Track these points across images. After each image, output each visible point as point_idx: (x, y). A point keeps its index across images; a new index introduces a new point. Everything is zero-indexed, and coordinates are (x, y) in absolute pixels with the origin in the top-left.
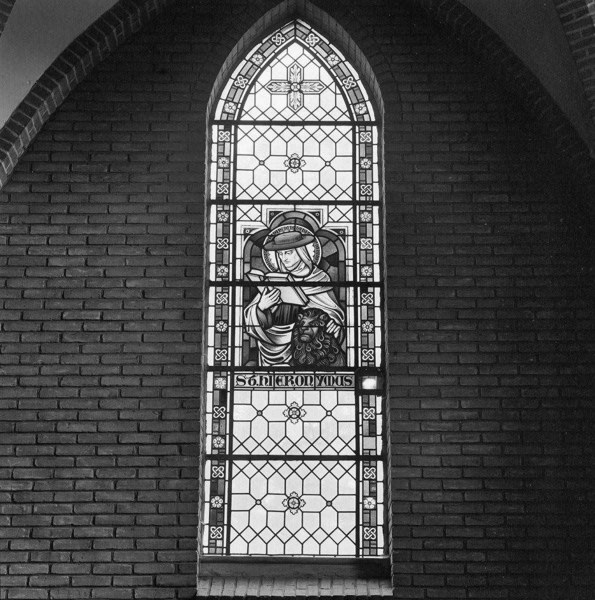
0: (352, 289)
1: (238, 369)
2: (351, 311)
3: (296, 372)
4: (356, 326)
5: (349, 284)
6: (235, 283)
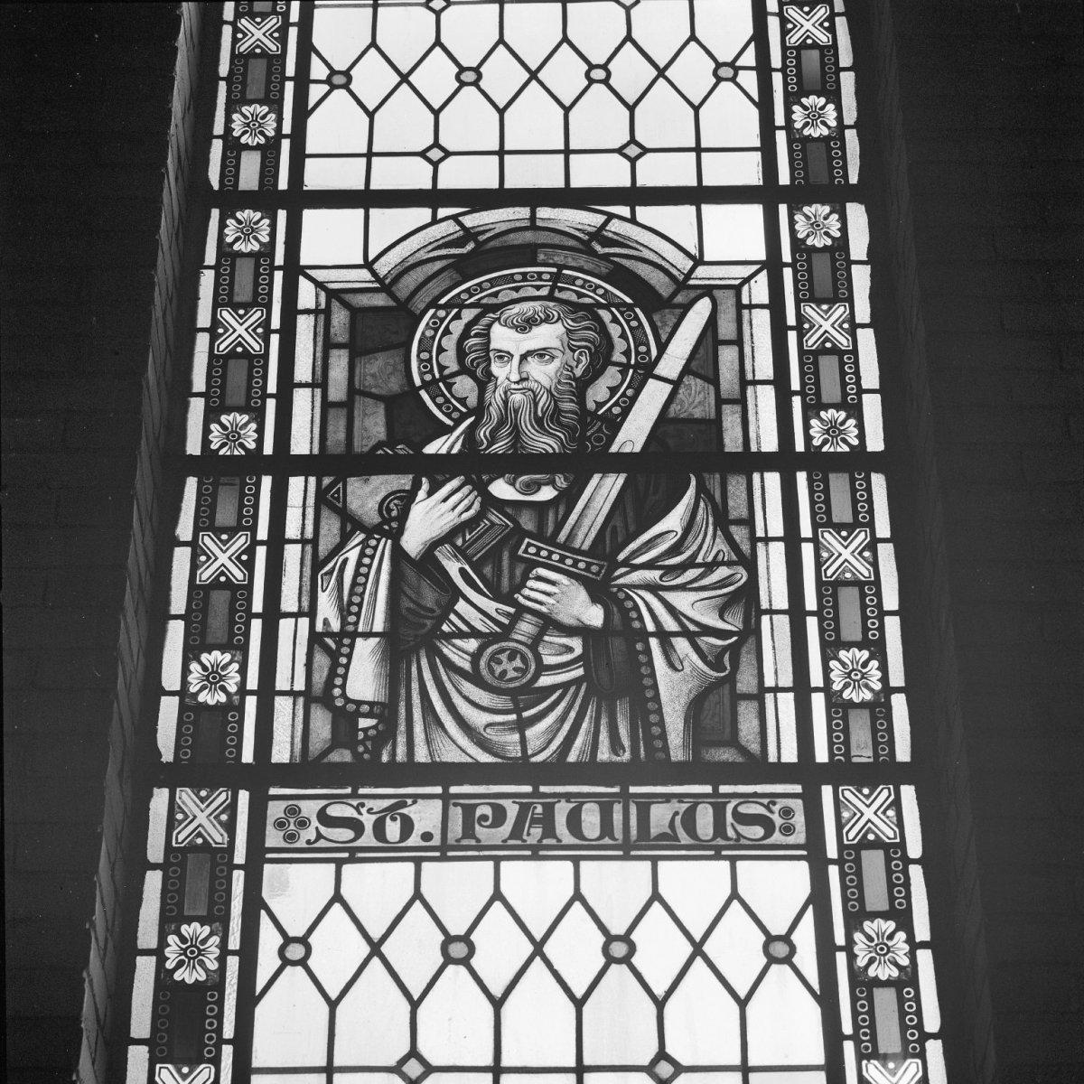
0: (773, 480)
1: (287, 774)
2: (773, 561)
3: (543, 789)
4: (796, 612)
5: (764, 462)
6: (284, 465)
